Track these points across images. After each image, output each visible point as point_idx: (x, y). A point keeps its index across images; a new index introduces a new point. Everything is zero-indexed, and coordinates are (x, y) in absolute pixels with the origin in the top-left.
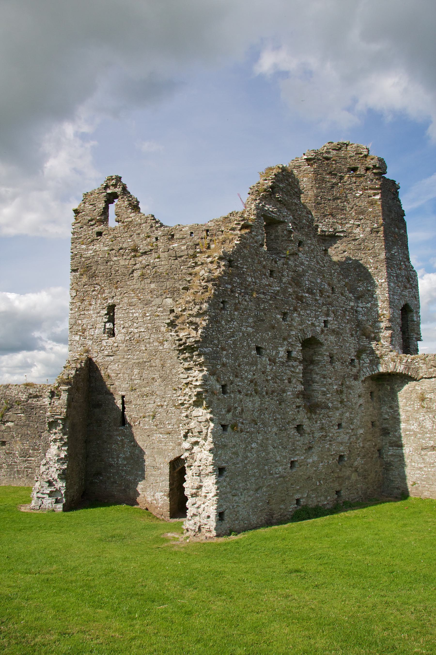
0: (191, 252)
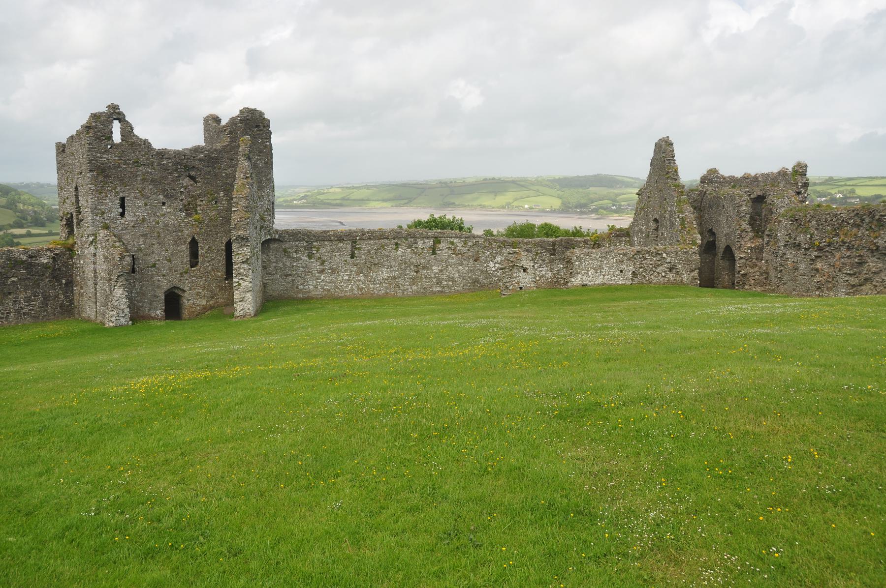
0: (174, 167)
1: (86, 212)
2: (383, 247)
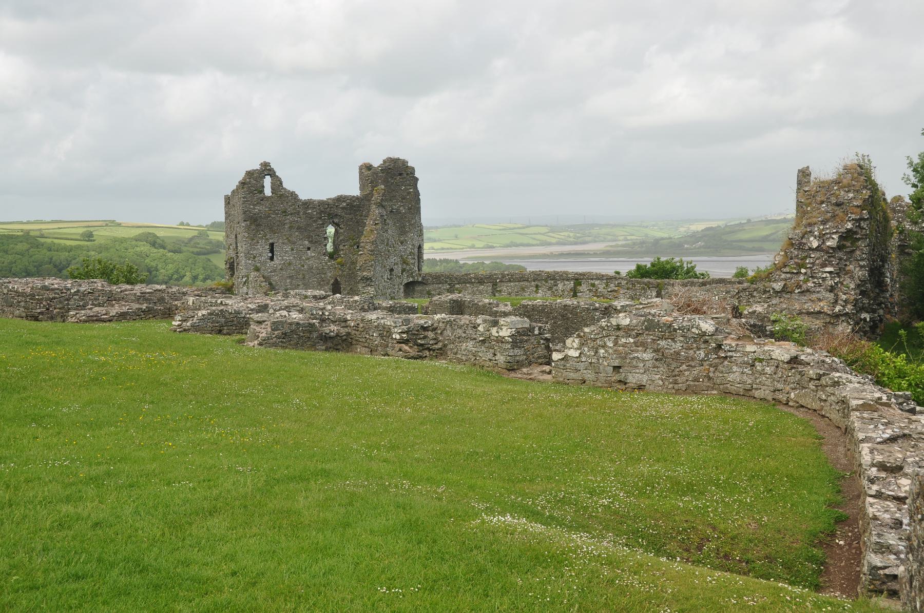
2: (523, 289)
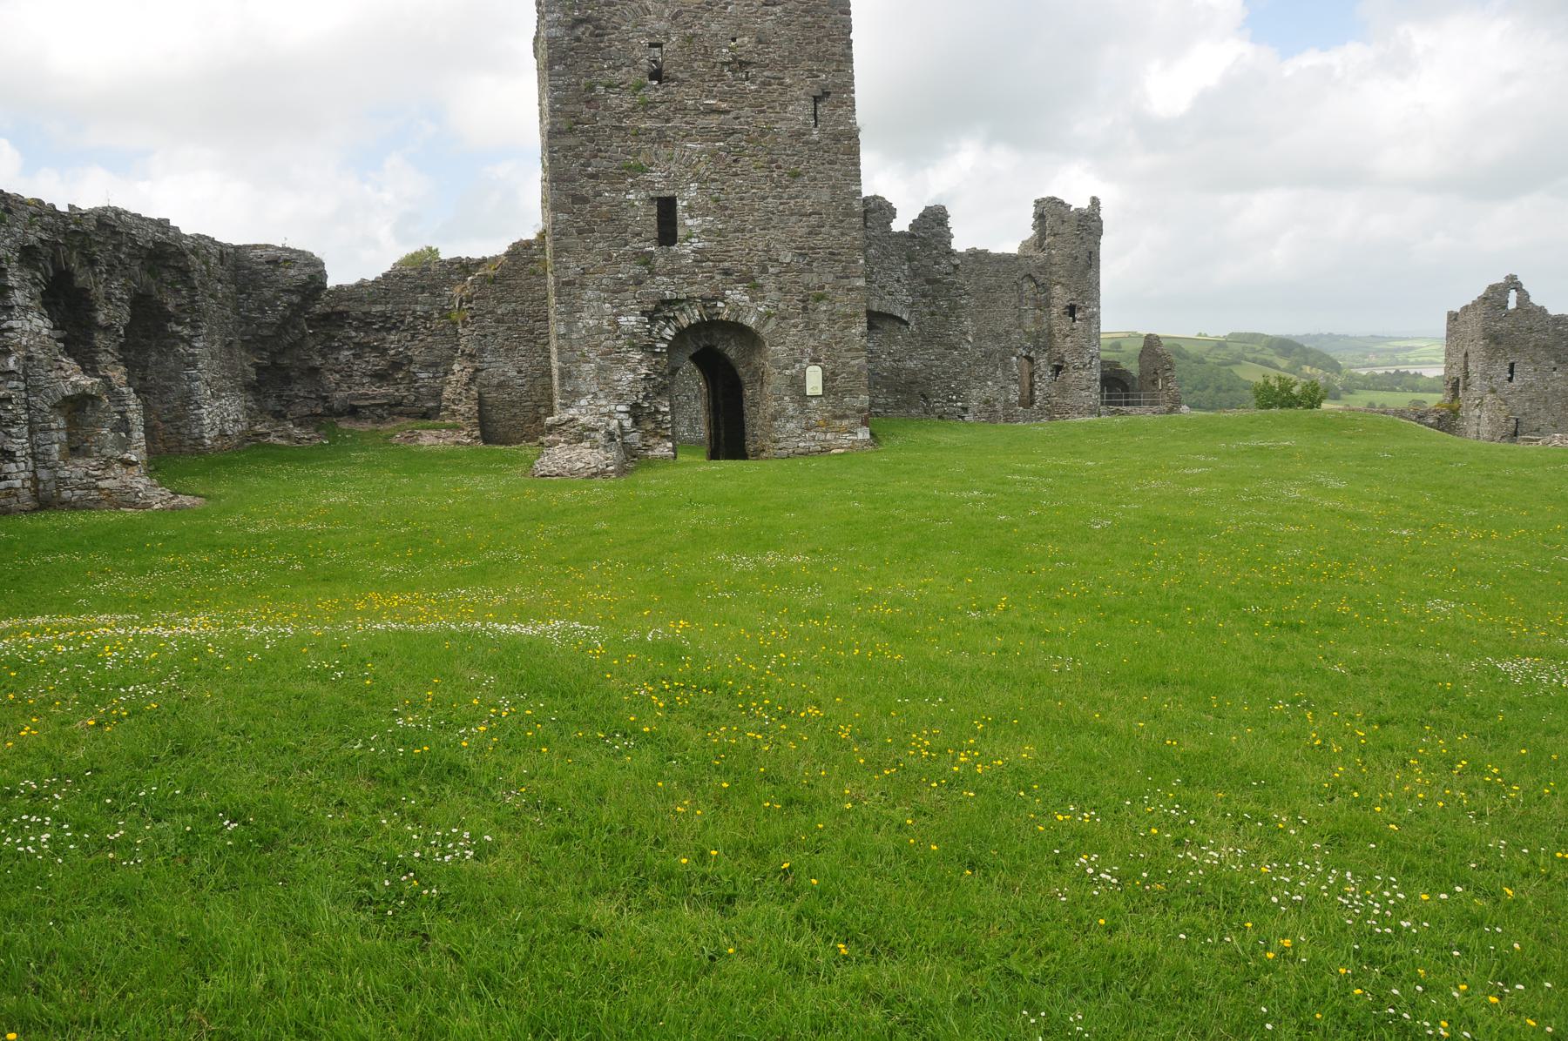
1: (1475, 377)
